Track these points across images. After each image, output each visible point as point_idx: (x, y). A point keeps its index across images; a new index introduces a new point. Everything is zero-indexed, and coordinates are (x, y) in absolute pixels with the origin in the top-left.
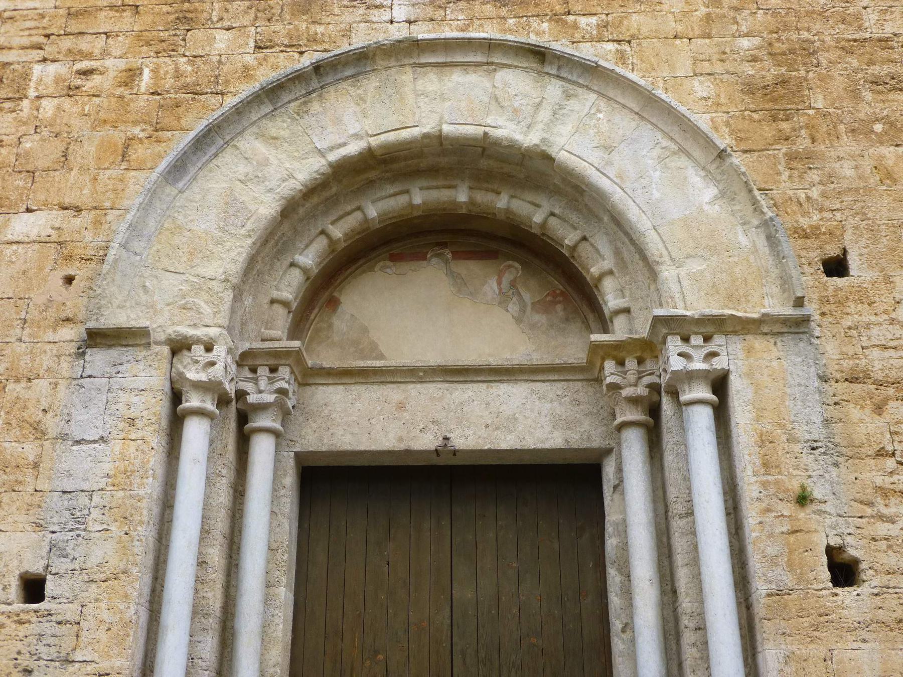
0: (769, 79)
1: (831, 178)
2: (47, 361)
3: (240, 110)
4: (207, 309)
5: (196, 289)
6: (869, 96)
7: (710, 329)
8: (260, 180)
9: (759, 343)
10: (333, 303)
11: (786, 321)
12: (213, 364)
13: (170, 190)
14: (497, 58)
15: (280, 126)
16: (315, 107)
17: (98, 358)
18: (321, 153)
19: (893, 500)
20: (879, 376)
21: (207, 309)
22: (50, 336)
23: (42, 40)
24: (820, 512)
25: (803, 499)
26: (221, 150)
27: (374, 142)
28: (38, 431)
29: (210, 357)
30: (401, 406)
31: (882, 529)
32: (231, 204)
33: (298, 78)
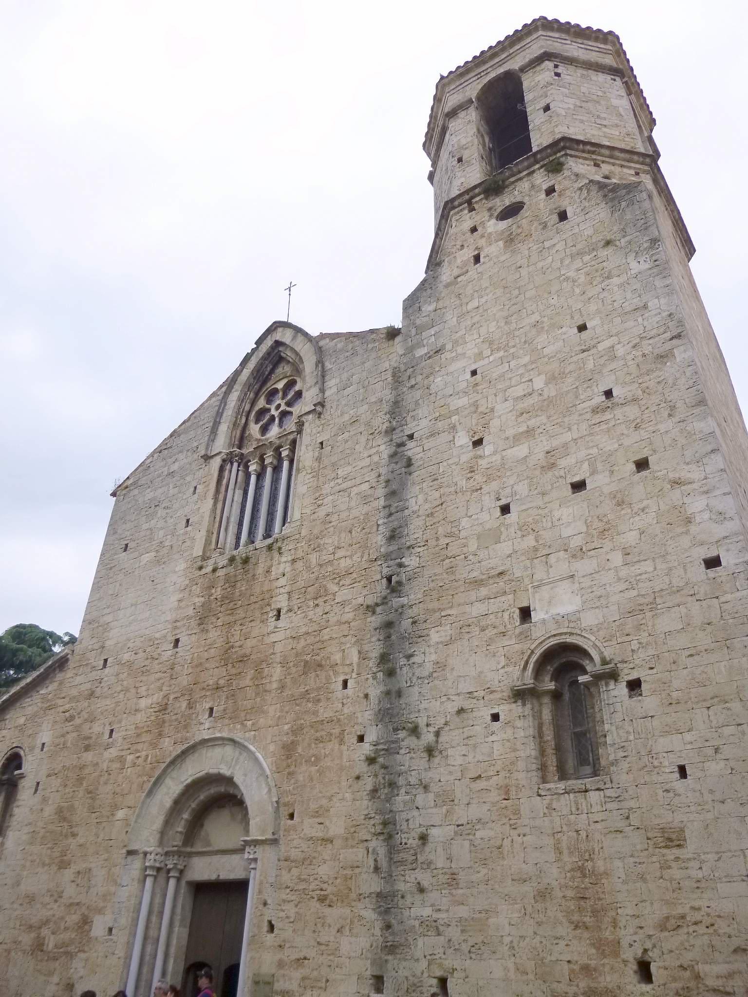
0: (289, 743)
1: (297, 781)
3: (165, 771)
6: (313, 745)
7: (254, 844)
9: (267, 847)
10: (202, 826)
11: (271, 840)
13: (148, 800)
14: (226, 742)
16: (183, 765)
17: (130, 858)
18: (182, 783)
19: (286, 903)
20: (292, 858)
23: (130, 746)
24: (268, 908)
25: (265, 904)
26: (161, 784)
28: (115, 882)
30: (210, 864)
31: (282, 914)
33: (178, 757)
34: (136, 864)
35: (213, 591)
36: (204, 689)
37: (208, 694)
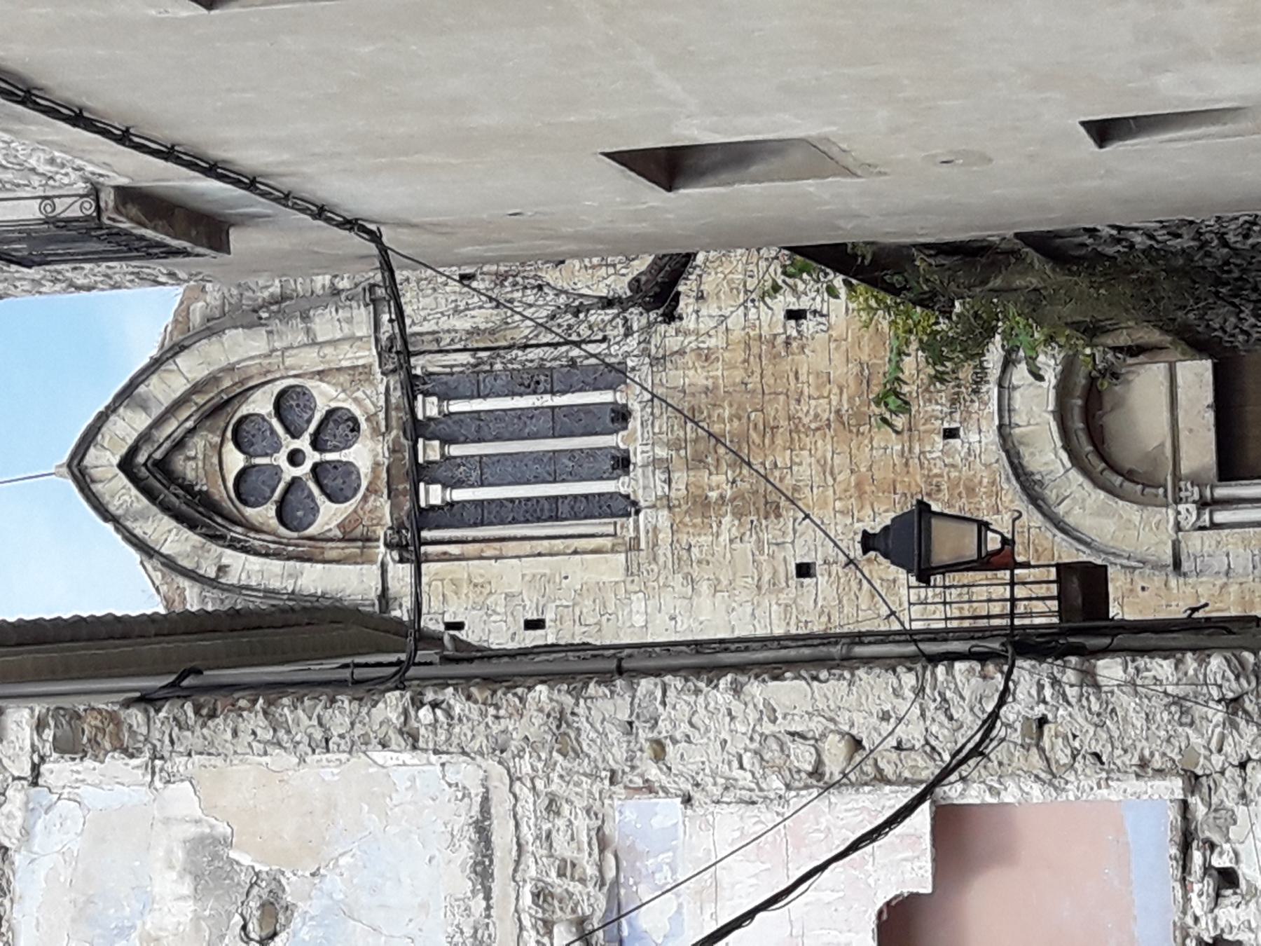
2: (1189, 590)
4: (1158, 517)
5: (1148, 523)
8: (1084, 500)
12: (1187, 510)
15: (1051, 494)
17: (1186, 566)
21: (1158, 517)
22: (1175, 591)
27: (1059, 444)
29: (1183, 512)
32: (1100, 512)
34: (1195, 543)
35: (714, 495)
36: (907, 464)
37: (917, 450)
